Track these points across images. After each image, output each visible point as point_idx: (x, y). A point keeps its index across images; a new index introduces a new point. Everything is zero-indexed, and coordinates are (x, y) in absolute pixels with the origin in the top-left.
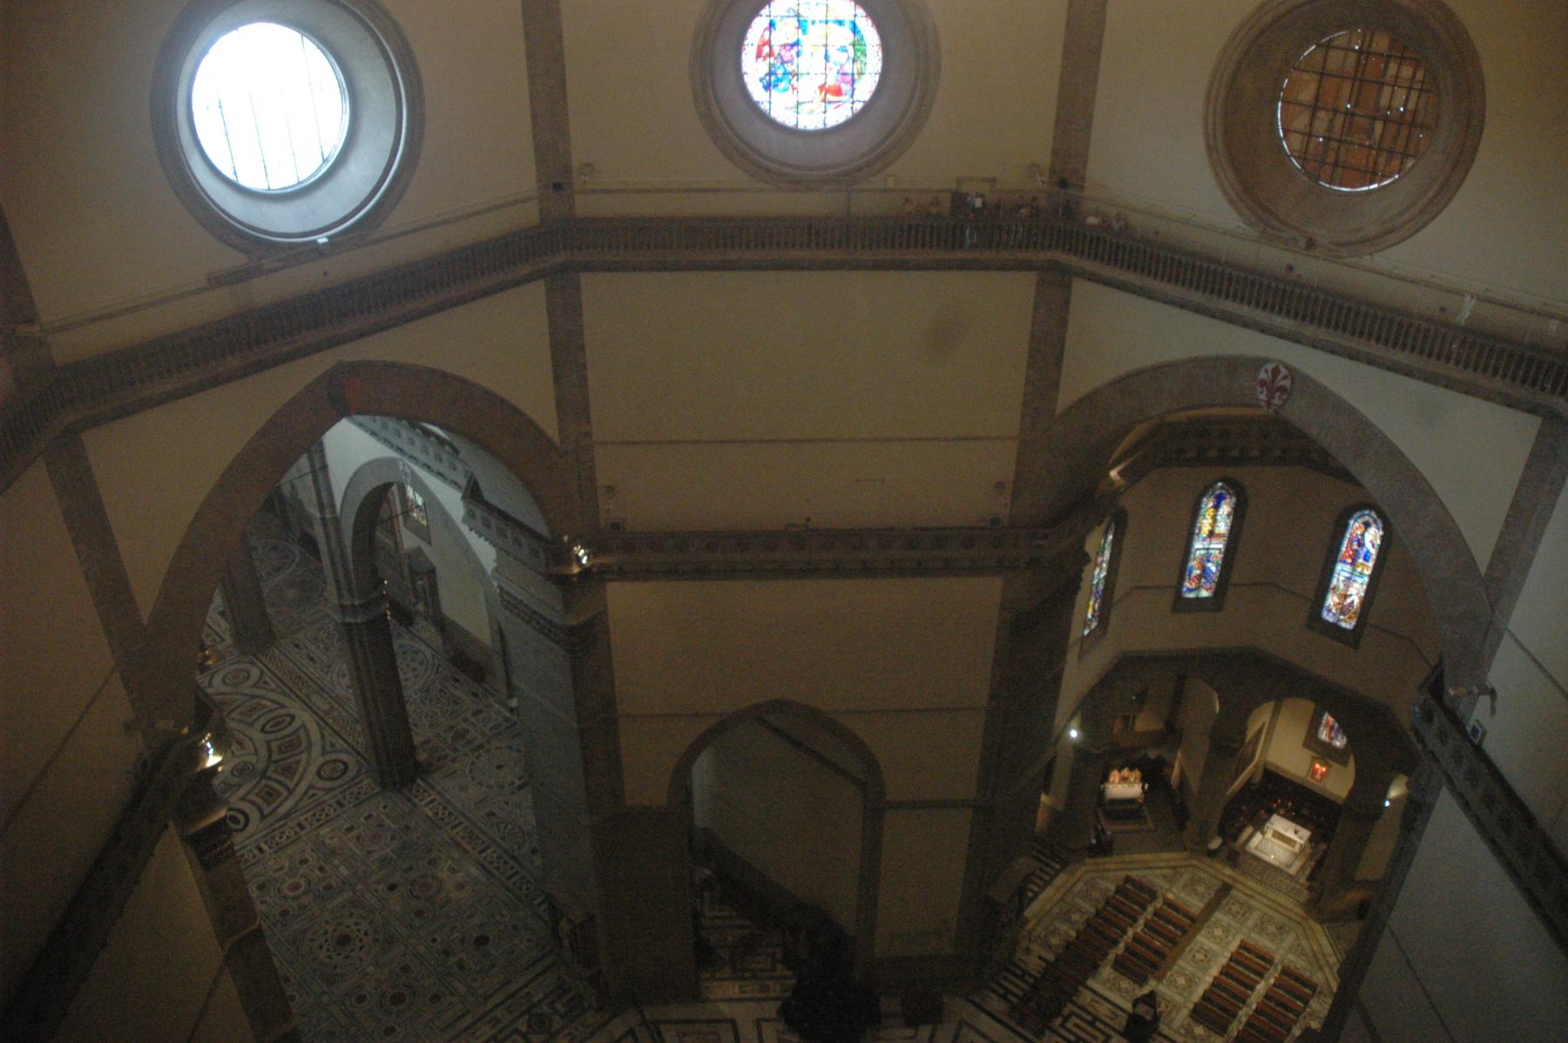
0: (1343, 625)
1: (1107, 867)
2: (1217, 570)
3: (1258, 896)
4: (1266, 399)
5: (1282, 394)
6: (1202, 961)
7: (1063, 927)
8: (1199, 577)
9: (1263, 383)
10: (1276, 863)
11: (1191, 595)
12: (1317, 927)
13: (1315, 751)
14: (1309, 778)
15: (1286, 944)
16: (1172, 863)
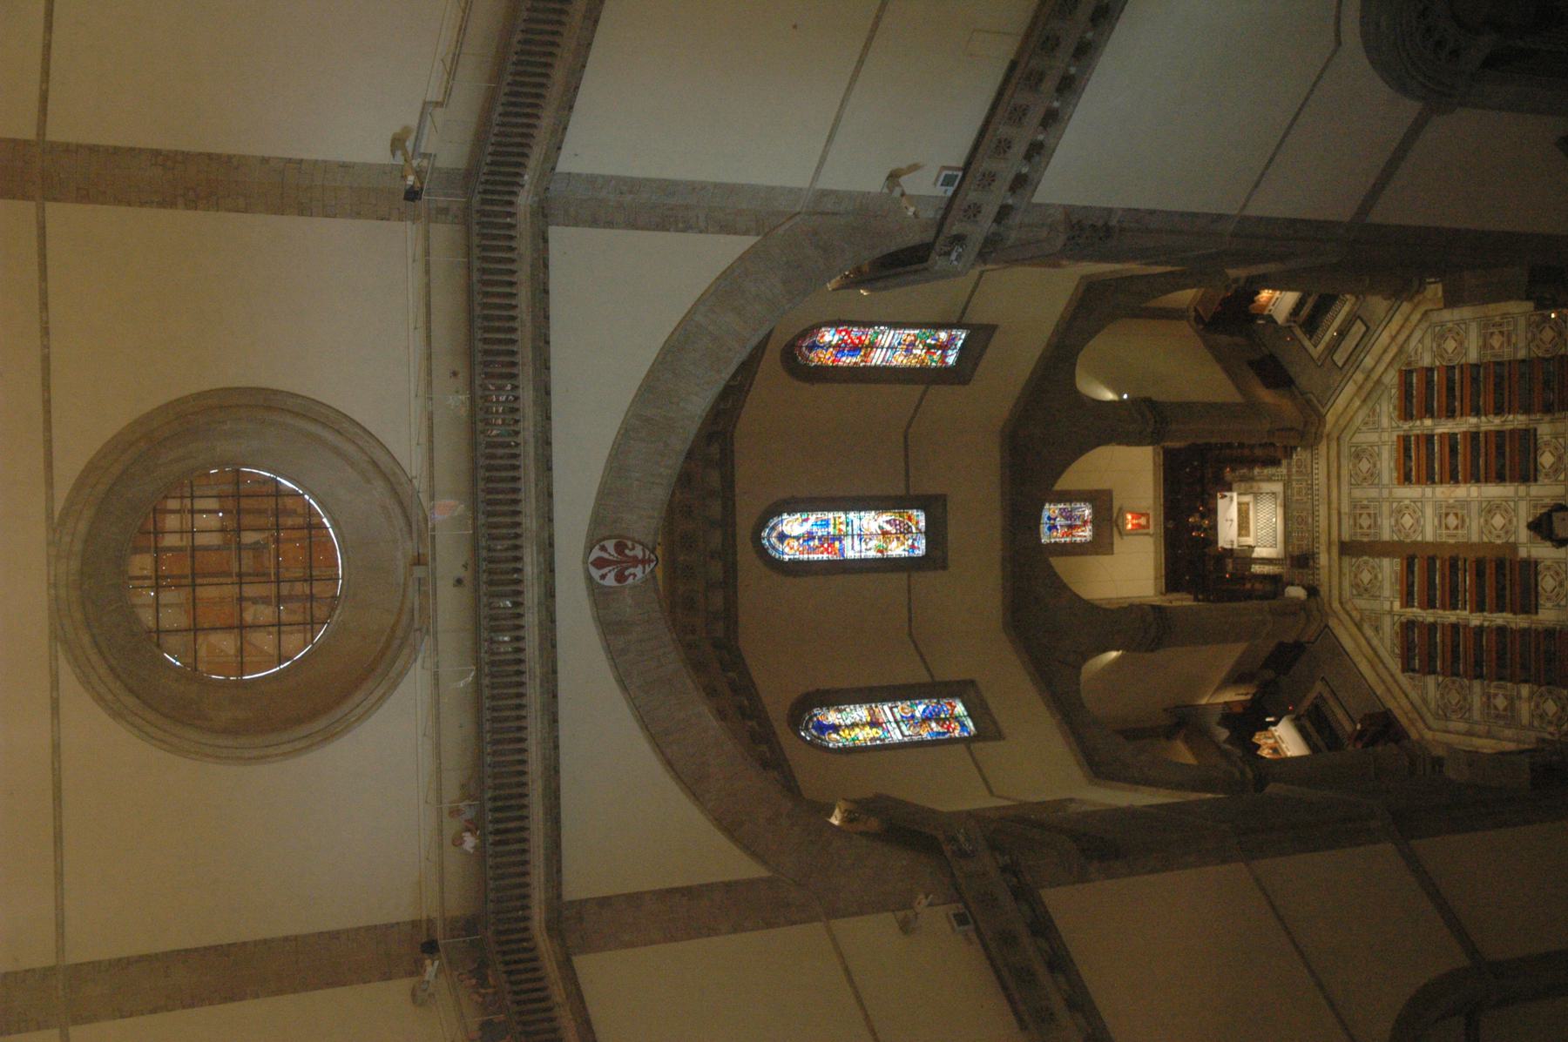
0: (922, 524)
1: (1407, 707)
2: (920, 703)
3: (1335, 505)
4: (640, 567)
5: (626, 546)
6: (1456, 515)
7: (1525, 710)
8: (938, 721)
9: (621, 578)
10: (1280, 511)
11: (969, 723)
12: (1330, 418)
13: (1111, 536)
14: (1151, 530)
15: (1373, 437)
16: (1354, 630)
